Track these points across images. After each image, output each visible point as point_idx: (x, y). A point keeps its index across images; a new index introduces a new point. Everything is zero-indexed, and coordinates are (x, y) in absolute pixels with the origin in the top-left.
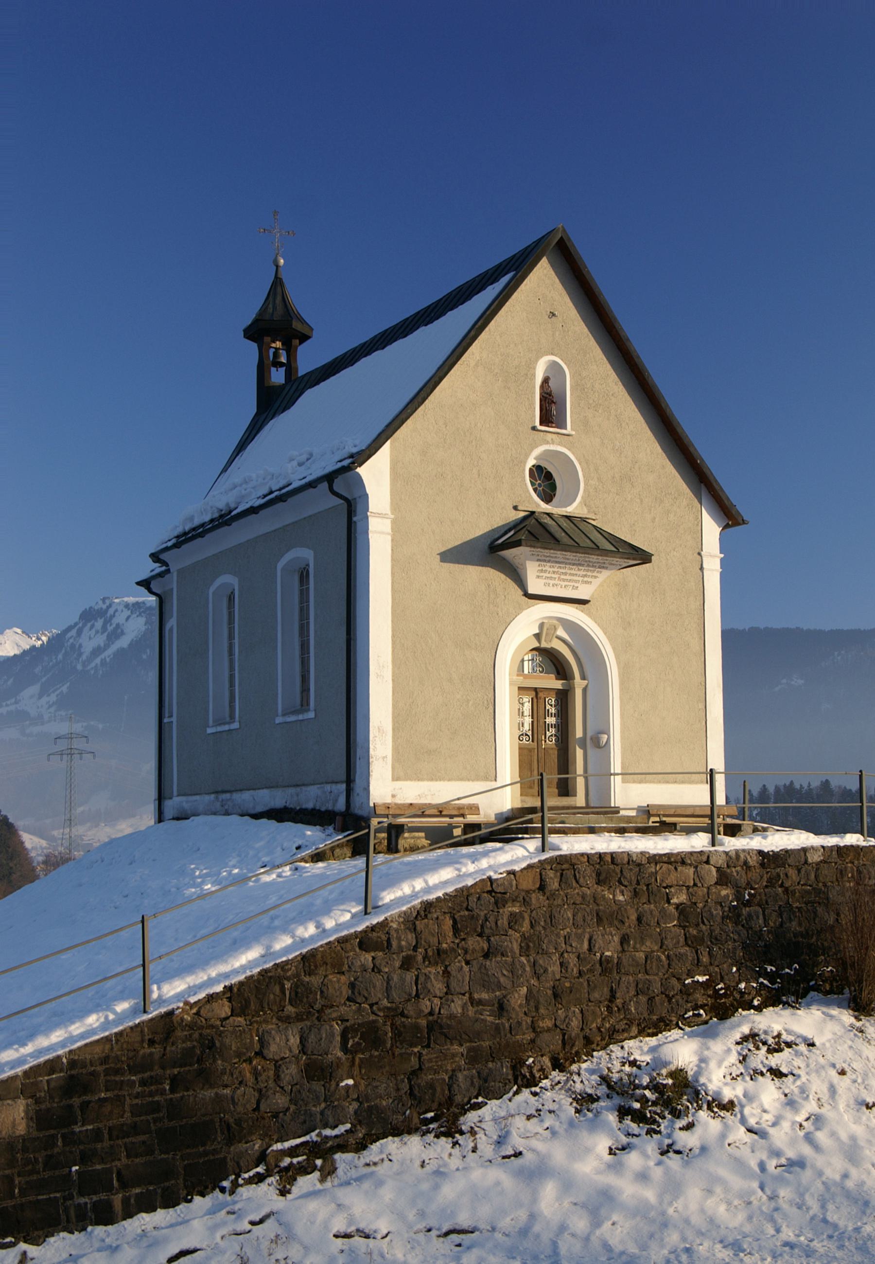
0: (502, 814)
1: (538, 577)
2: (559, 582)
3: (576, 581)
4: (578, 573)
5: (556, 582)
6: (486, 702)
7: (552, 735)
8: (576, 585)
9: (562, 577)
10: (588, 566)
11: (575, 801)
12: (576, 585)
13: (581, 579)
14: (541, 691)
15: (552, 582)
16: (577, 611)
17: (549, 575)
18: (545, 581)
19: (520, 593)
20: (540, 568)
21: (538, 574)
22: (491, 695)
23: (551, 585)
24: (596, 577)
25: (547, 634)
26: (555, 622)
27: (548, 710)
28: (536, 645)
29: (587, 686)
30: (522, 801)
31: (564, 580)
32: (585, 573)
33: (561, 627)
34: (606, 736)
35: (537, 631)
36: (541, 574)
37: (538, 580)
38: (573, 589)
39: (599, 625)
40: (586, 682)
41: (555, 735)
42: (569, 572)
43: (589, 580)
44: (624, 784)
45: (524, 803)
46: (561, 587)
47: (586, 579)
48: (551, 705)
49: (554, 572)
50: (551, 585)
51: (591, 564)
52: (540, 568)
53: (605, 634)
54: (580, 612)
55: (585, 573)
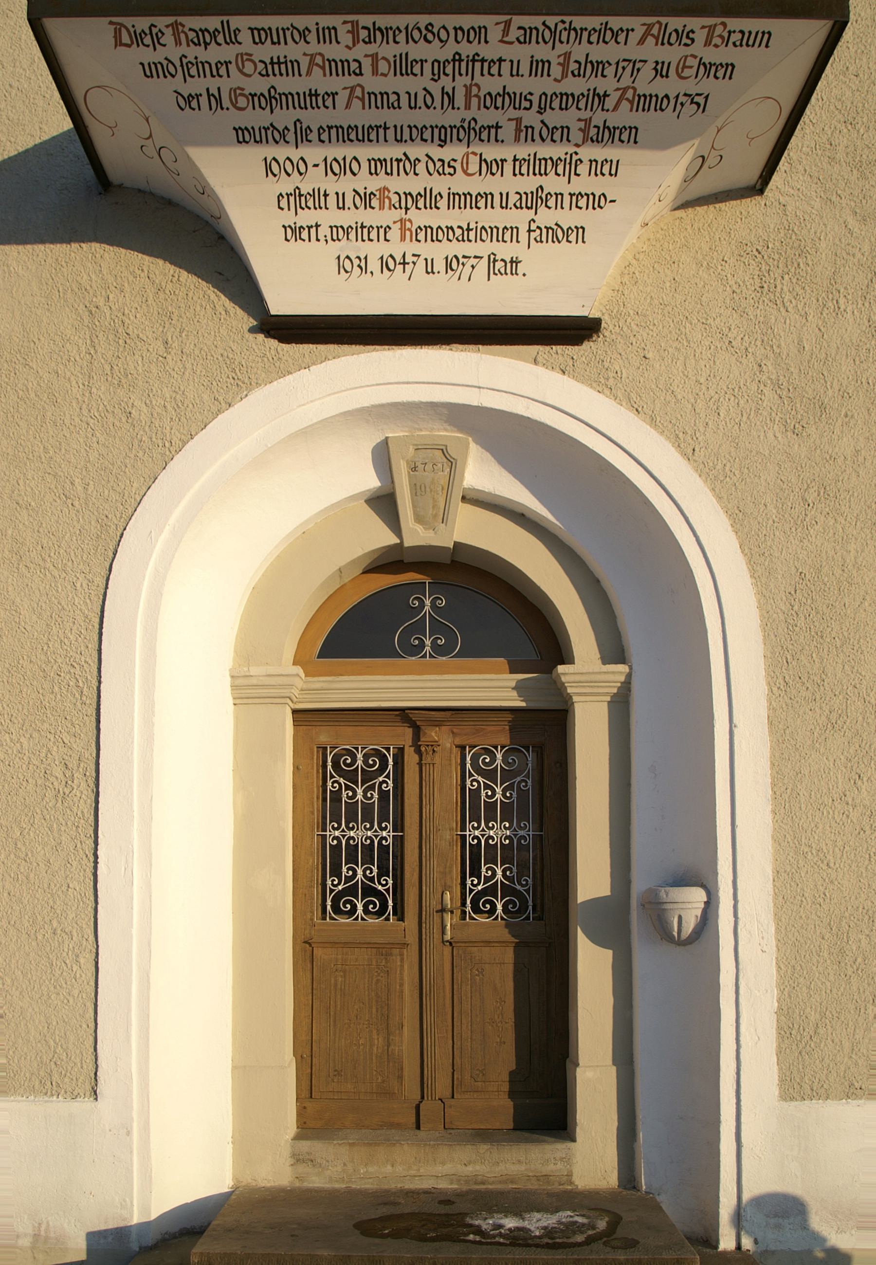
0: (121, 1234)
1: (295, 232)
2: (411, 248)
3: (497, 233)
4: (494, 184)
5: (396, 247)
6: (58, 771)
7: (491, 891)
8: (505, 251)
9: (419, 217)
10: (524, 133)
11: (567, 1160)
12: (505, 251)
13: (520, 218)
14: (438, 724)
15: (374, 250)
16: (539, 370)
17: (347, 218)
18: (335, 248)
19: (244, 321)
20: (286, 185)
21: (288, 217)
22: (83, 745)
23: (374, 265)
24: (597, 201)
25: (417, 489)
26: (445, 433)
27: (476, 793)
28: (386, 538)
29: (626, 687)
30: (298, 1159)
31: (433, 234)
32: (529, 184)
33: (474, 449)
34: (698, 896)
35: (372, 482)
36: (306, 218)
37: (295, 246)
38: (491, 271)
39: (653, 421)
40: (623, 668)
41: (507, 890)
42: (440, 184)
43: (568, 218)
44: (785, 1104)
45: (302, 1168)
46: (430, 270)
47: (546, 217)
48: (490, 775)
49: (366, 199)
50: (374, 265)
51: (531, 118)
52: (286, 185)
53: (689, 455)
54: (557, 376)
55: (529, 184)
